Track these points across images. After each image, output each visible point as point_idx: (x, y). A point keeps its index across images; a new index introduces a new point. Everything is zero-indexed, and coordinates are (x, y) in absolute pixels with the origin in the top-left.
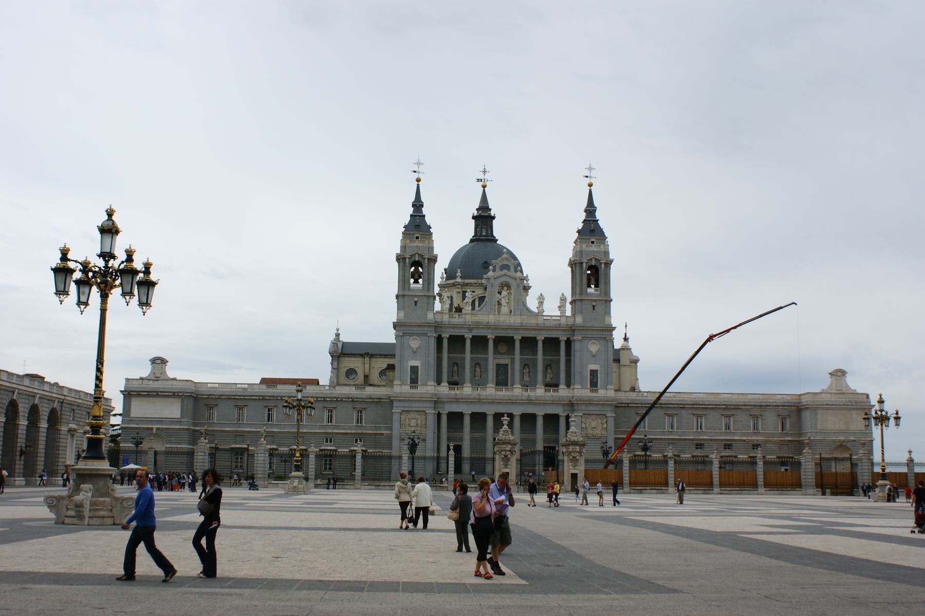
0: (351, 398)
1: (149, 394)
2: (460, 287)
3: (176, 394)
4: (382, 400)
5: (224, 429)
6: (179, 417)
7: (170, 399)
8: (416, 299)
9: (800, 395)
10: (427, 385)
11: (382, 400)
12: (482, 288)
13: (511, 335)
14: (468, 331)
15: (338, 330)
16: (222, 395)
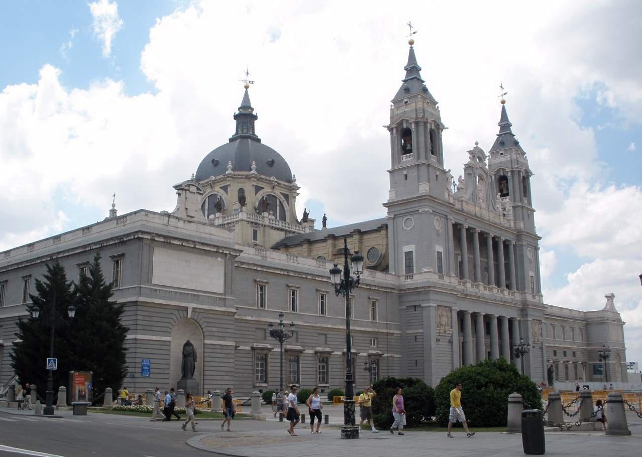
0: (370, 285)
1: (182, 245)
2: (256, 180)
3: (221, 251)
4: (392, 291)
5: (245, 318)
6: (222, 292)
7: (210, 259)
8: (438, 173)
9: (585, 313)
10: (450, 276)
11: (392, 291)
12: (269, 185)
13: (488, 231)
14: (464, 220)
15: (114, 205)
16: (243, 263)
